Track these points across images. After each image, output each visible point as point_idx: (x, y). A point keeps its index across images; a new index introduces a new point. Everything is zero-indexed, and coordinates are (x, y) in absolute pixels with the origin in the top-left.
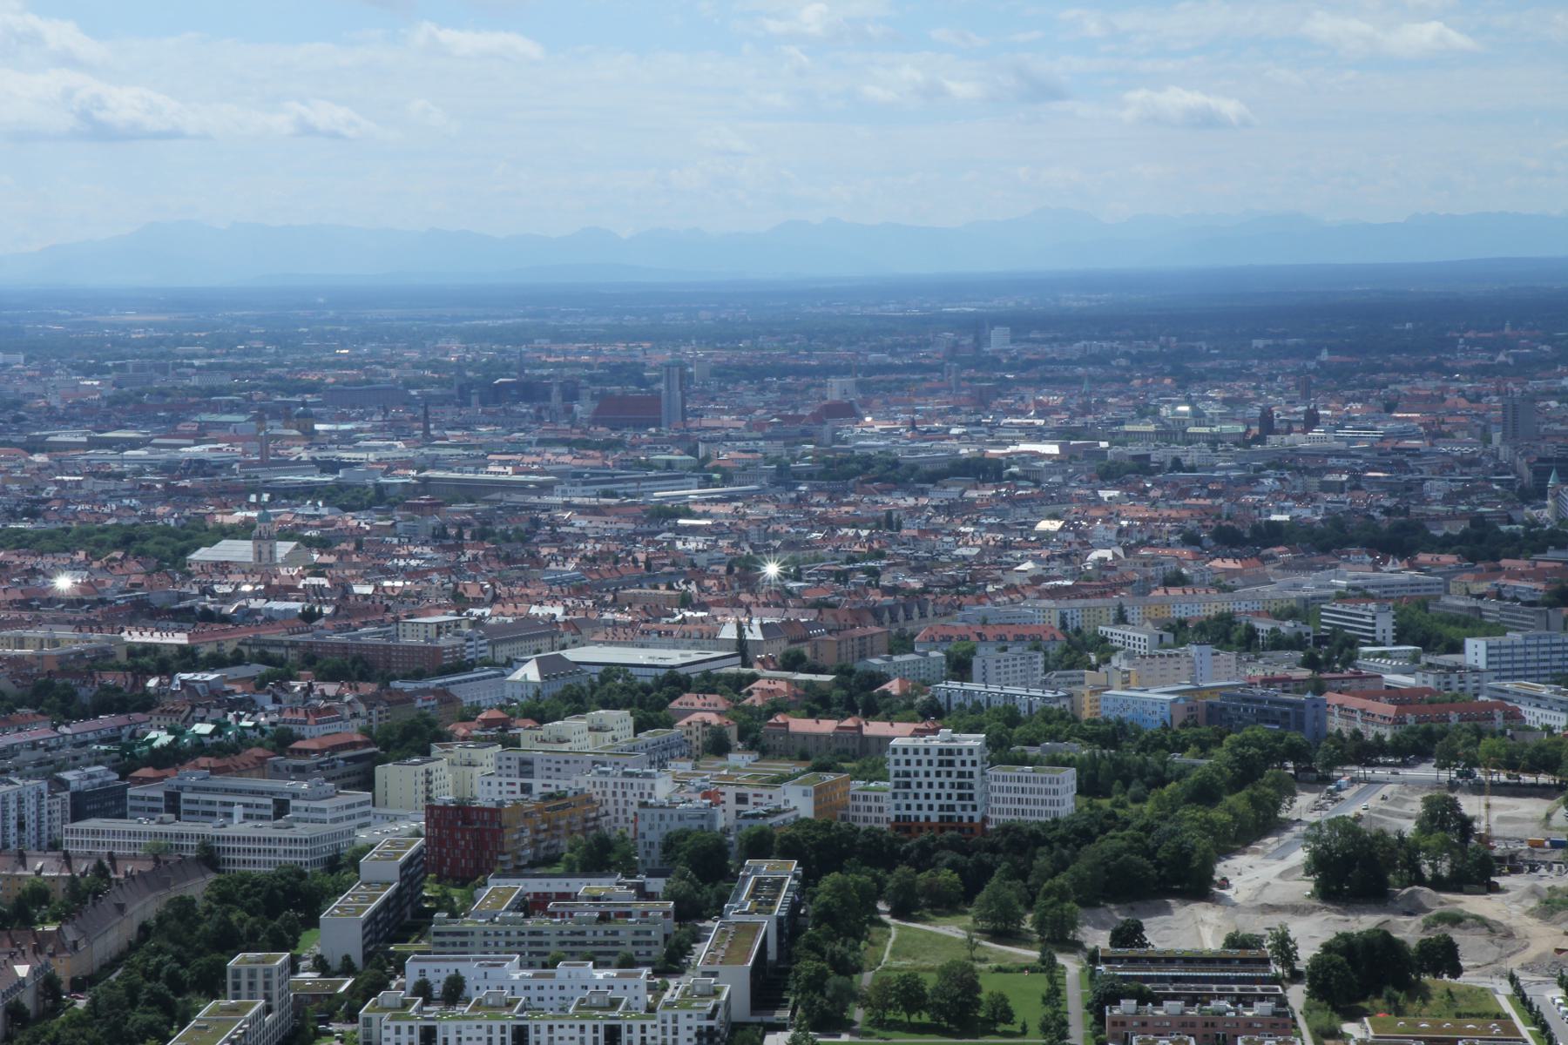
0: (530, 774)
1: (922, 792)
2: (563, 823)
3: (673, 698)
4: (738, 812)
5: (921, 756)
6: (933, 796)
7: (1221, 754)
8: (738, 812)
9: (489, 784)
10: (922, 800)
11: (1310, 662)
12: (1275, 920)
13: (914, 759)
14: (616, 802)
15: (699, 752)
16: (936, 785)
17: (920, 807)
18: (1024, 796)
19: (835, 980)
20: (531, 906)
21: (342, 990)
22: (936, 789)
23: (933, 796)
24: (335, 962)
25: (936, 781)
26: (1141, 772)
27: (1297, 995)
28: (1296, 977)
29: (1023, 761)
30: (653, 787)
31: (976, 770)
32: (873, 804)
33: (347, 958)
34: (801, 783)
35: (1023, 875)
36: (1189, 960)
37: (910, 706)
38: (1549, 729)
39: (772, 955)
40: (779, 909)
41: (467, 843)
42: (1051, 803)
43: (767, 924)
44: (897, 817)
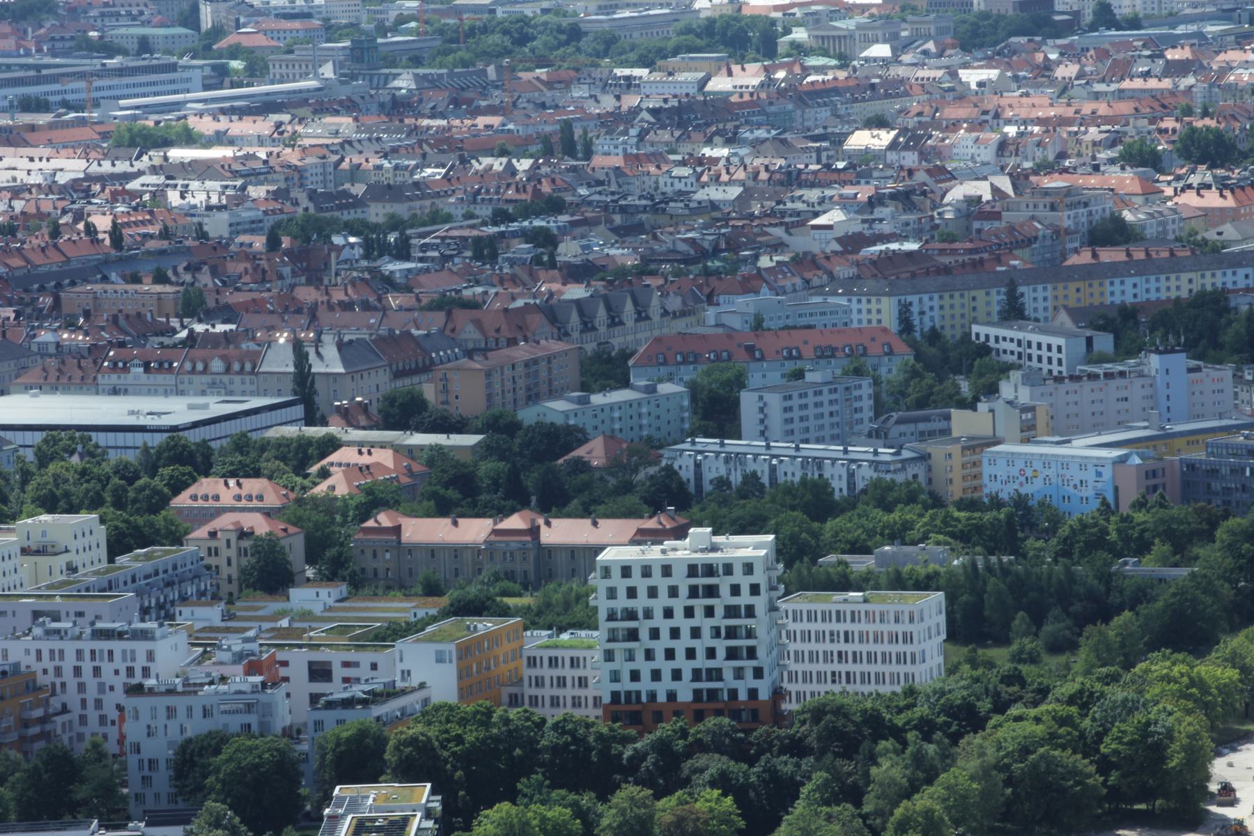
1: (659, 647)
3: (178, 487)
4: (314, 698)
5: (657, 579)
6: (680, 654)
7: (1211, 556)
8: (314, 698)
10: (660, 662)
13: (642, 585)
14: (81, 687)
15: (234, 588)
16: (685, 633)
17: (656, 675)
18: (849, 648)
22: (685, 641)
23: (680, 654)
25: (685, 625)
26: (1064, 593)
29: (844, 583)
30: (150, 656)
31: (760, 603)
32: (568, 672)
34: (431, 639)
35: (855, 795)
42: (902, 658)
44: (615, 696)
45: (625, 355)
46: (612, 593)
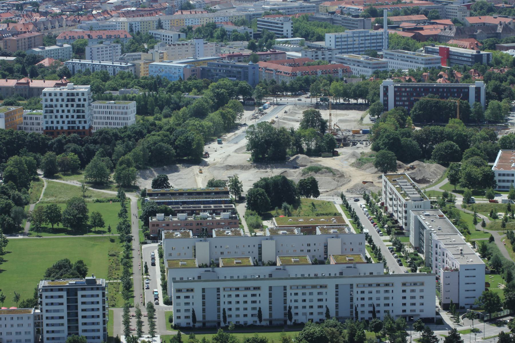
1: (59, 115)
5: (58, 97)
6: (64, 117)
7: (208, 93)
10: (59, 119)
11: (252, 47)
12: (232, 173)
13: (54, 98)
16: (66, 111)
17: (58, 122)
18: (110, 116)
19: (15, 208)
22: (66, 113)
23: (64, 117)
25: (66, 109)
26: (168, 102)
27: (241, 209)
28: (241, 200)
29: (111, 99)
31: (86, 103)
32: (35, 121)
35: (110, 155)
36: (190, 194)
37: (54, 72)
38: (364, 78)
44: (47, 127)
45: (55, 37)
46: (46, 100)
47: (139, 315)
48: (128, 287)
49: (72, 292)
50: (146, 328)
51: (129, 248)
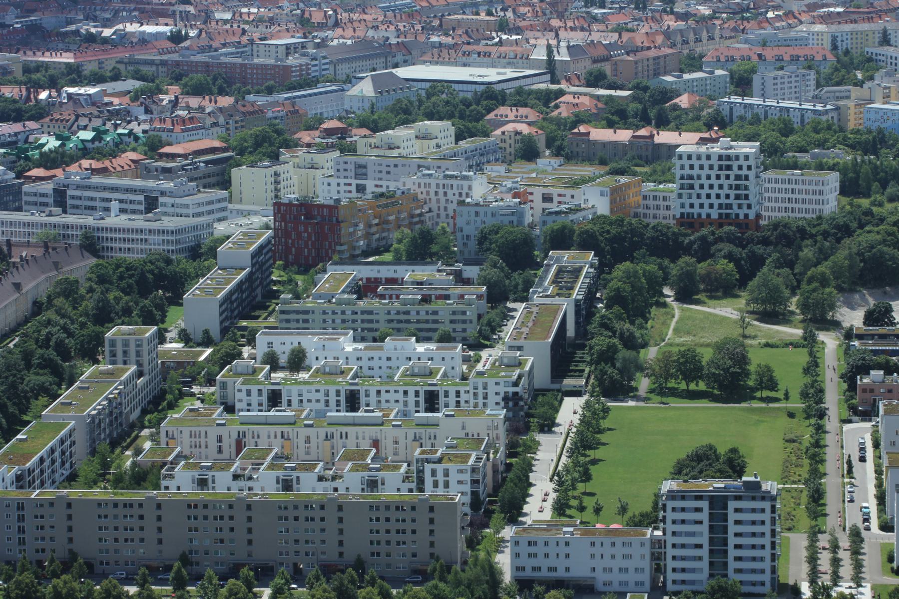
0: (364, 176)
1: (704, 192)
2: (392, 218)
3: (489, 111)
4: (544, 210)
6: (713, 196)
8: (544, 210)
9: (329, 184)
10: (704, 200)
13: (697, 164)
14: (438, 201)
15: (512, 158)
16: (716, 187)
17: (702, 206)
18: (794, 196)
19: (624, 354)
20: (365, 289)
21: (202, 358)
22: (716, 190)
23: (713, 196)
24: (198, 336)
25: (716, 183)
29: (795, 166)
30: (470, 188)
31: (751, 174)
32: (662, 203)
33: (206, 332)
34: (598, 185)
35: (791, 265)
37: (698, 118)
39: (571, 331)
40: (578, 293)
41: (309, 234)
42: (817, 202)
43: (566, 306)
44: (682, 214)
46: (682, 167)
47: (835, 547)
48: (817, 496)
49: (718, 502)
50: (846, 570)
51: (820, 429)
